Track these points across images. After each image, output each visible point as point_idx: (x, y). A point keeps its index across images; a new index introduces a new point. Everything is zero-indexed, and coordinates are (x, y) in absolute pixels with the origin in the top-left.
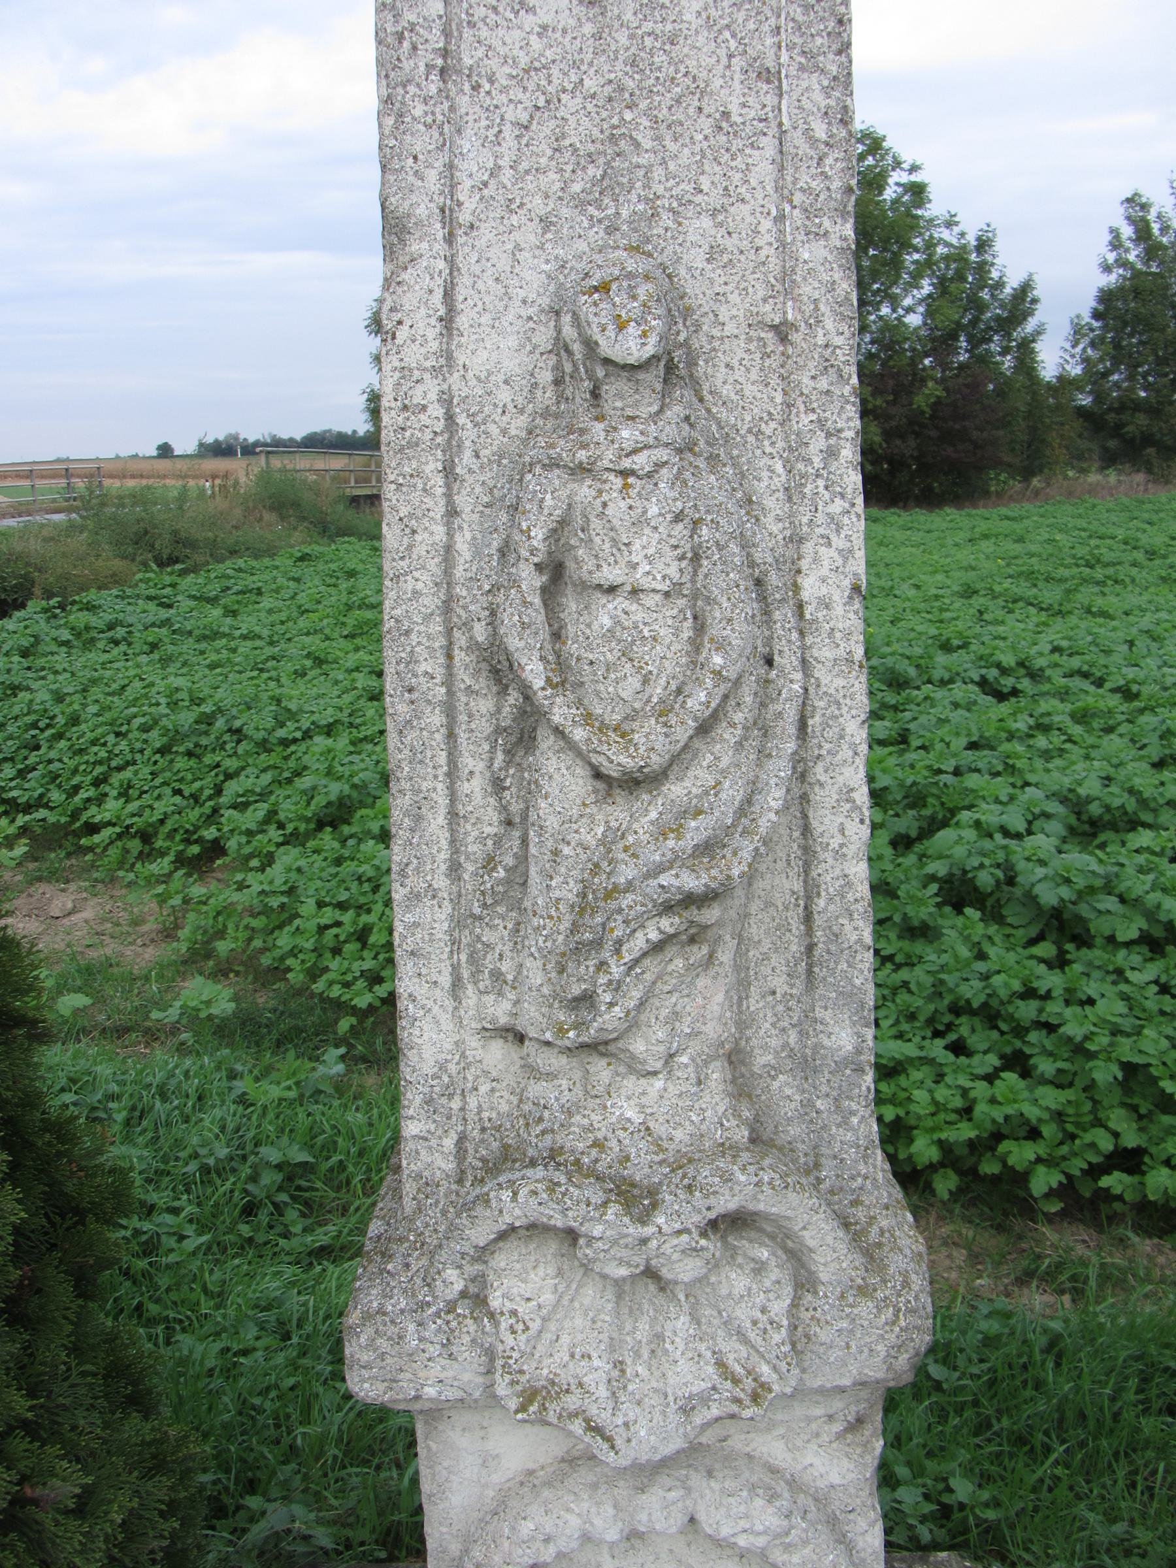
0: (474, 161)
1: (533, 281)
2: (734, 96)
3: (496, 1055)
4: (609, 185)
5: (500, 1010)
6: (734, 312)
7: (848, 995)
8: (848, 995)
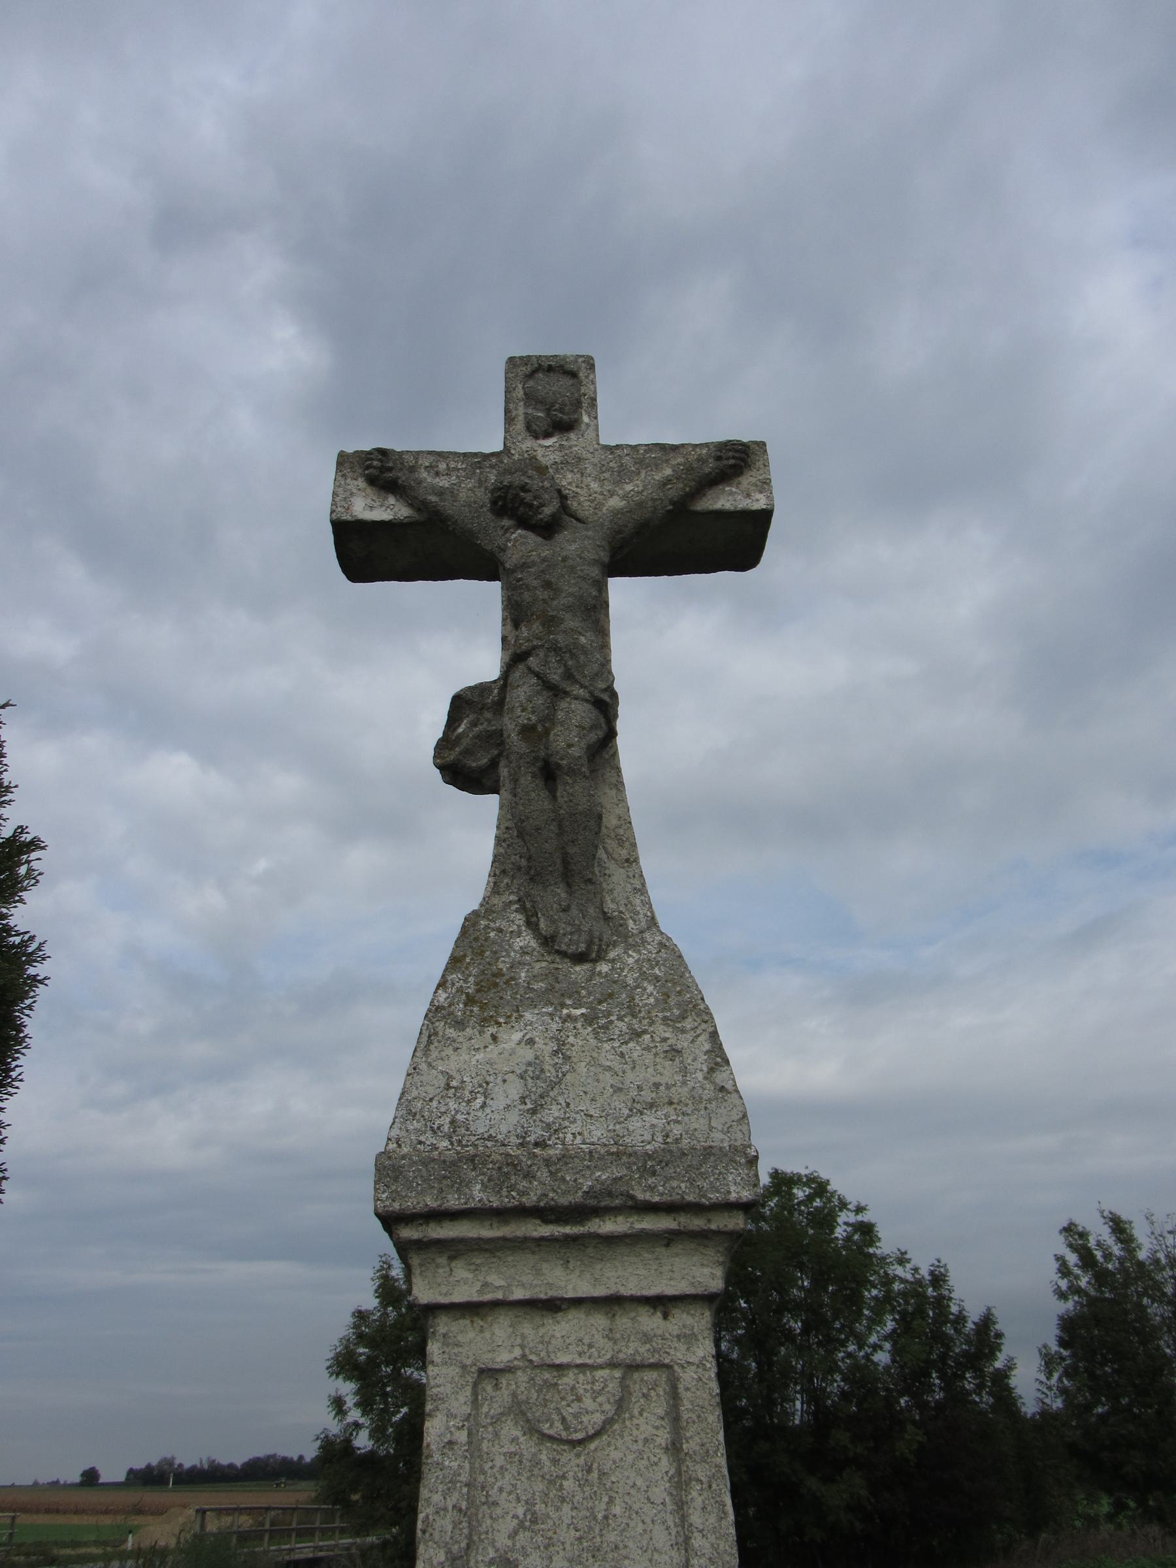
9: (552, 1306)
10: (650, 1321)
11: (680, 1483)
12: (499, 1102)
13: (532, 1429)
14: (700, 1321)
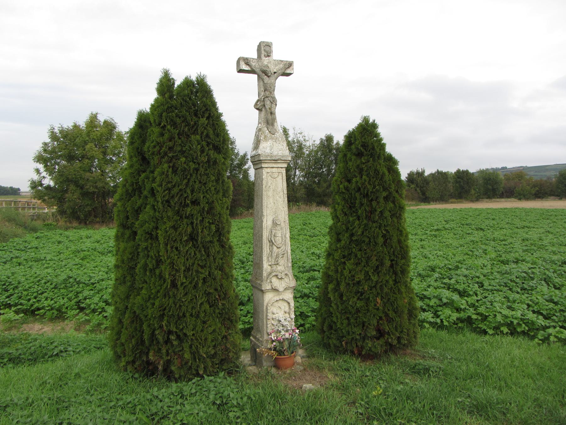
1: (271, 219)
3: (269, 267)
5: (270, 264)
9: (273, 167)
14: (285, 169)
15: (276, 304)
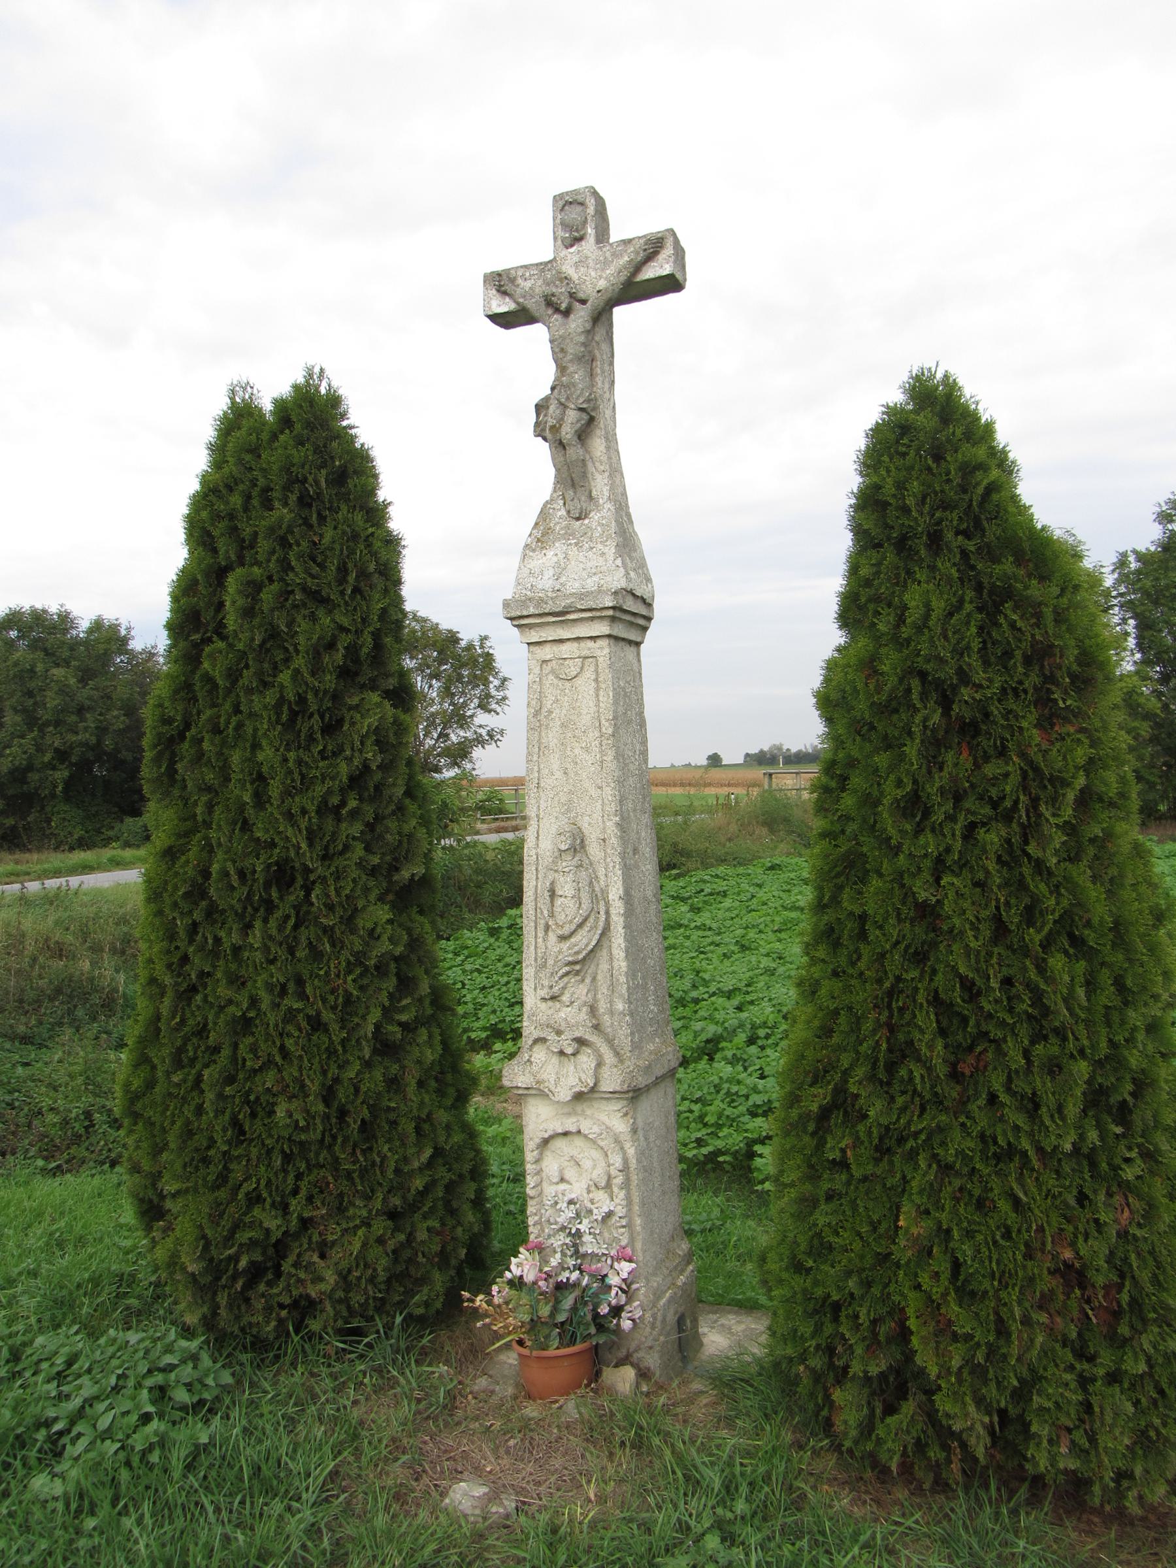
0: (542, 806)
1: (554, 830)
2: (593, 792)
4: (568, 810)
6: (594, 836)
7: (621, 996)
8: (621, 996)
9: (561, 641)
10: (590, 644)
11: (597, 689)
12: (546, 577)
13: (557, 677)
15: (560, 1143)
